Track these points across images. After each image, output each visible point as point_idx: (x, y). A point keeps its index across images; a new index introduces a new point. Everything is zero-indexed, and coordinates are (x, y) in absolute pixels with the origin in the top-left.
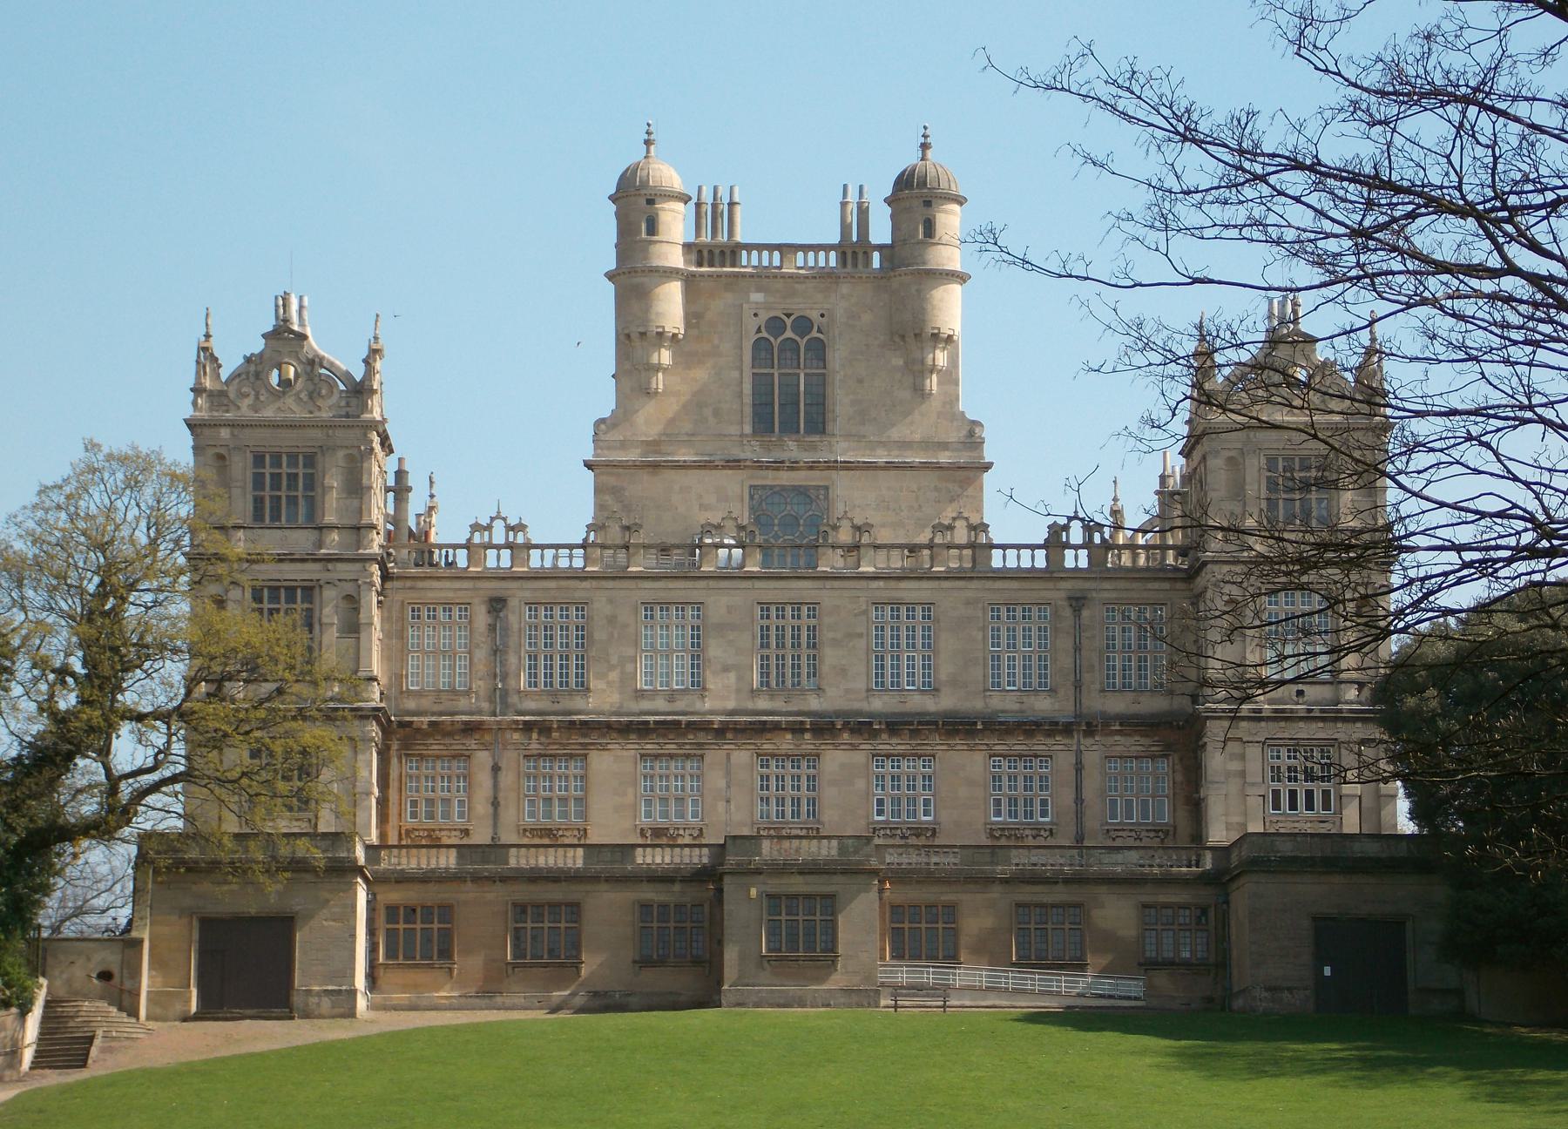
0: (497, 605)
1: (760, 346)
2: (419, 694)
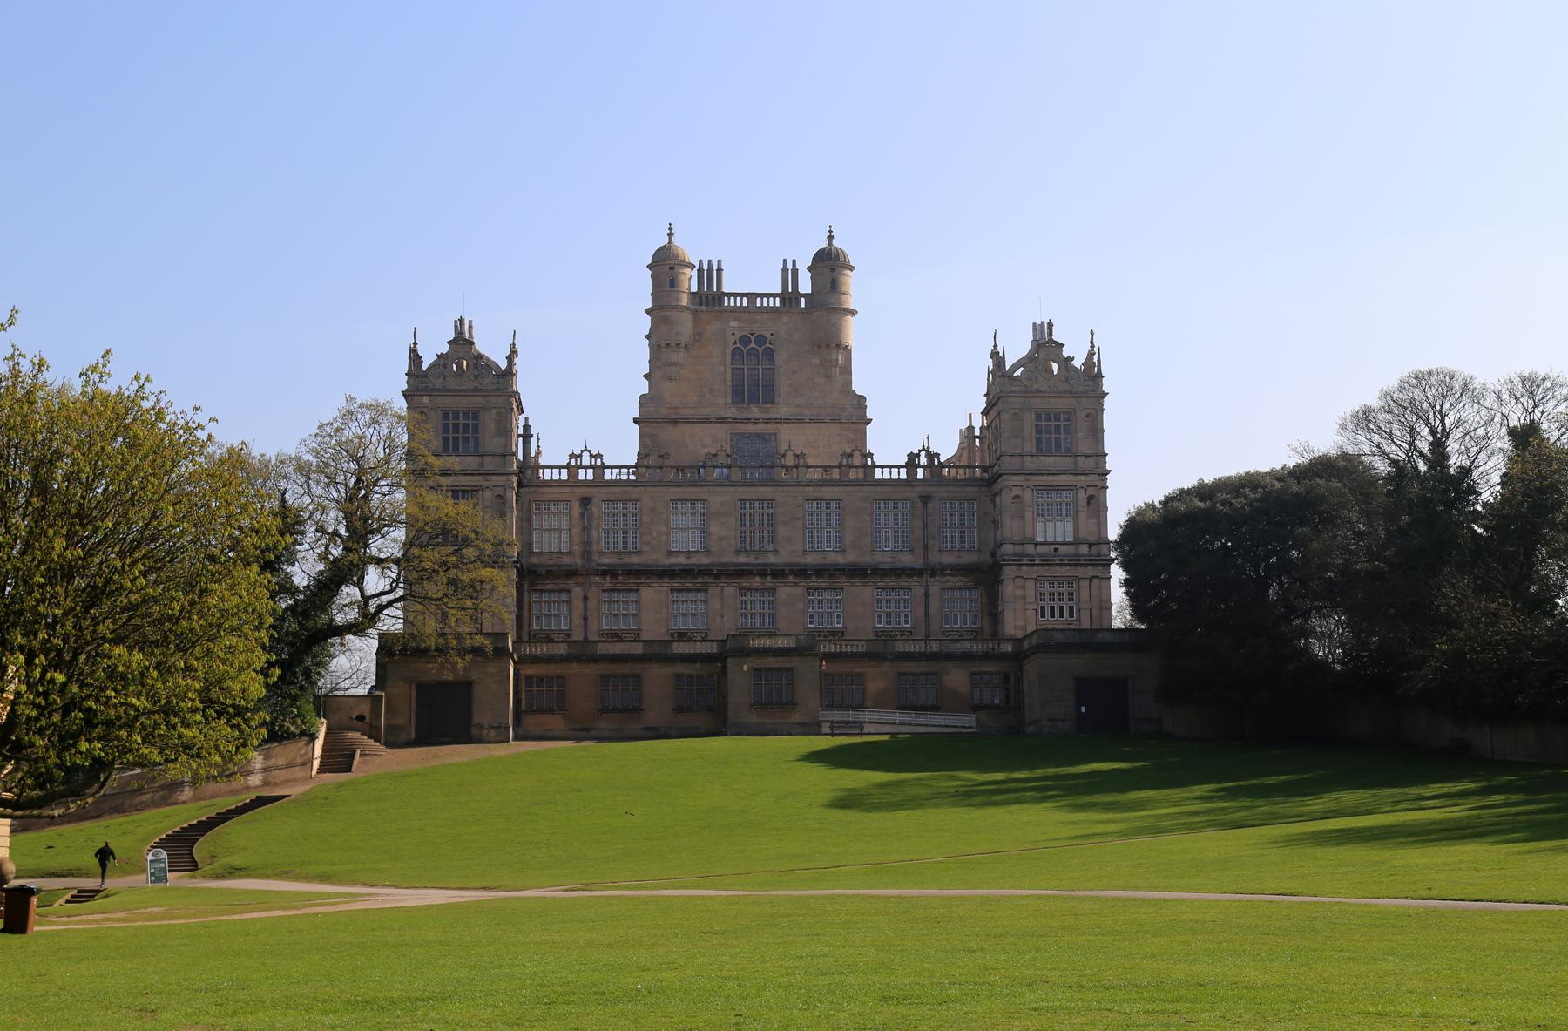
0: (585, 501)
2: (541, 553)
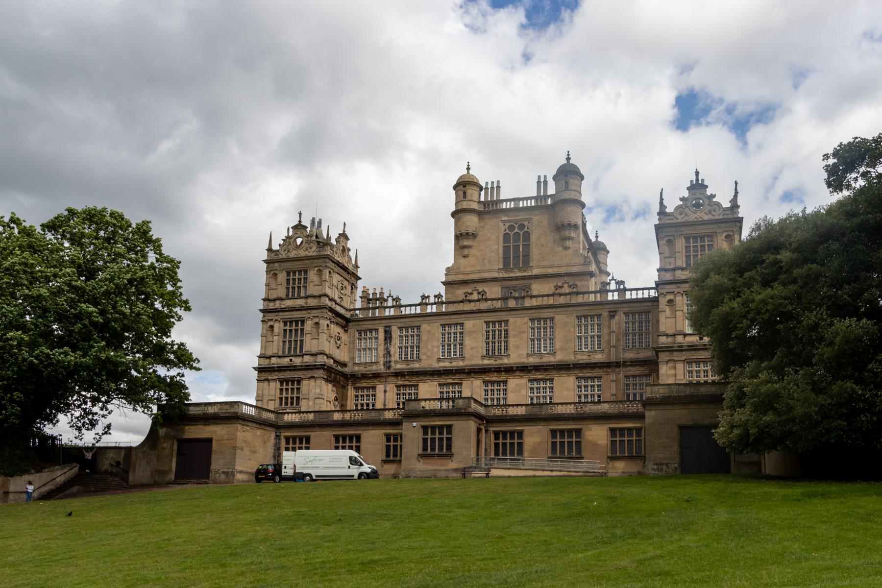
1: (506, 236)
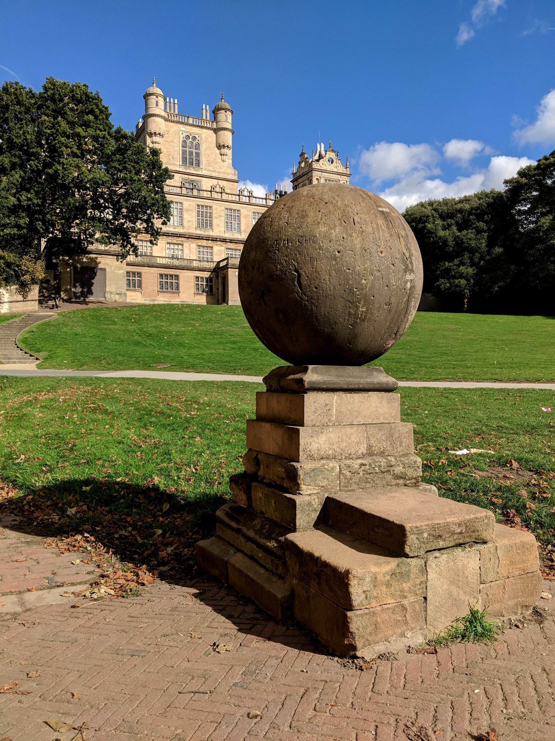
1: (184, 142)
